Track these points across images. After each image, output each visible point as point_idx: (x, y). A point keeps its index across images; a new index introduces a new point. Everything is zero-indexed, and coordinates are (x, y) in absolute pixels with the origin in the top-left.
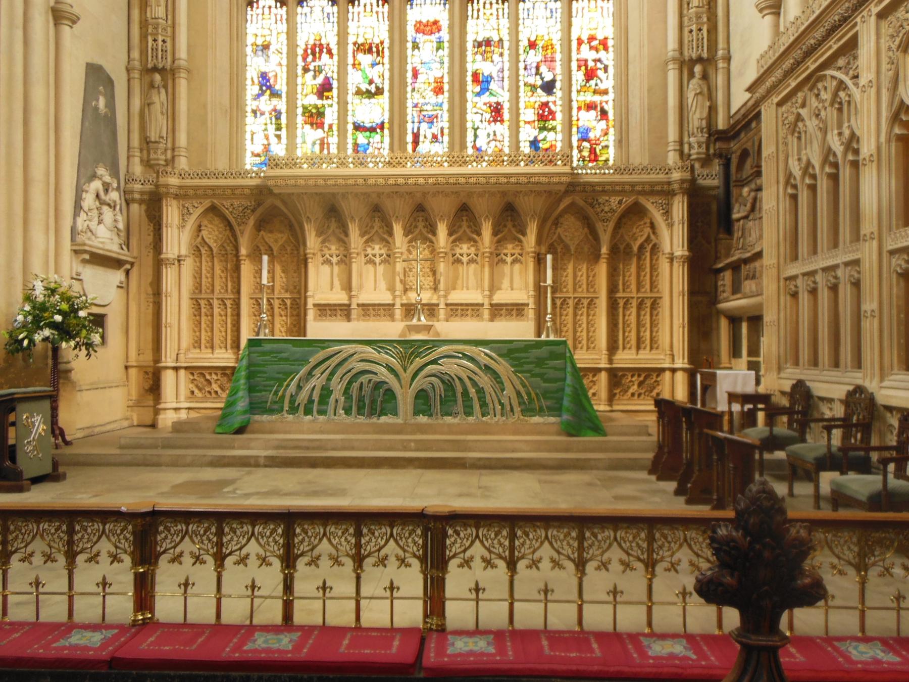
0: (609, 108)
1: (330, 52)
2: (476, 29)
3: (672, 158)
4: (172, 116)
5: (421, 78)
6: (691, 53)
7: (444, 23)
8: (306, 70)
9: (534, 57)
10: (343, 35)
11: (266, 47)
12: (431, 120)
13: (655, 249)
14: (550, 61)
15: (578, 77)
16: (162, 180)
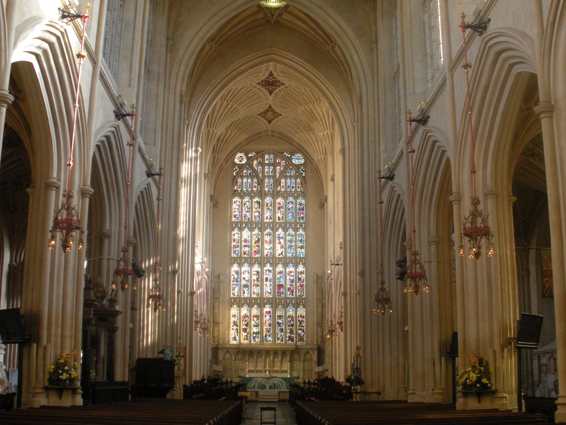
0: (304, 330)
1: (248, 317)
2: (278, 313)
3: (315, 343)
4: (219, 332)
5: (267, 323)
6: (318, 322)
7: (271, 312)
8: (243, 321)
9: (289, 319)
10: (250, 314)
11: (235, 315)
12: (269, 332)
13: (312, 360)
14: (293, 320)
15: (299, 323)
16: (219, 346)
